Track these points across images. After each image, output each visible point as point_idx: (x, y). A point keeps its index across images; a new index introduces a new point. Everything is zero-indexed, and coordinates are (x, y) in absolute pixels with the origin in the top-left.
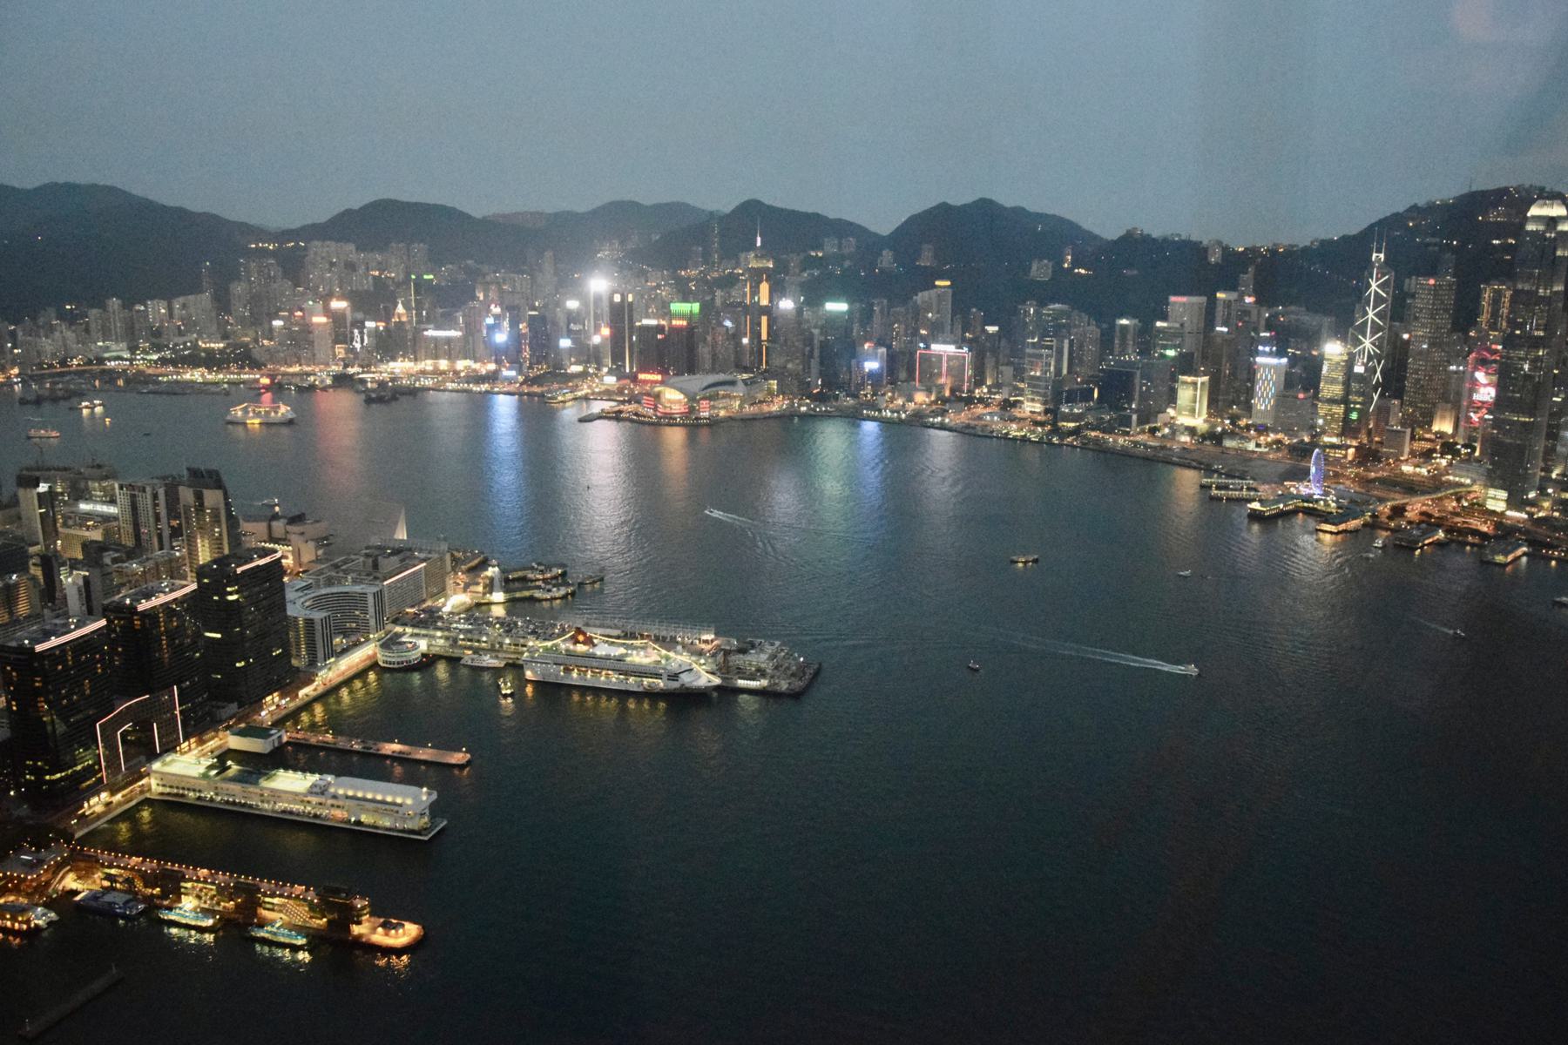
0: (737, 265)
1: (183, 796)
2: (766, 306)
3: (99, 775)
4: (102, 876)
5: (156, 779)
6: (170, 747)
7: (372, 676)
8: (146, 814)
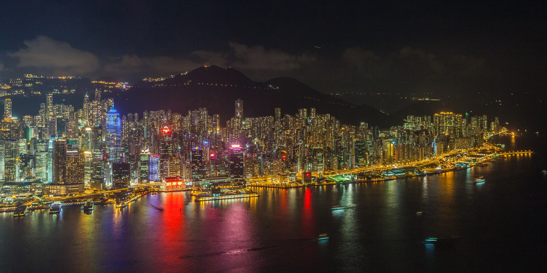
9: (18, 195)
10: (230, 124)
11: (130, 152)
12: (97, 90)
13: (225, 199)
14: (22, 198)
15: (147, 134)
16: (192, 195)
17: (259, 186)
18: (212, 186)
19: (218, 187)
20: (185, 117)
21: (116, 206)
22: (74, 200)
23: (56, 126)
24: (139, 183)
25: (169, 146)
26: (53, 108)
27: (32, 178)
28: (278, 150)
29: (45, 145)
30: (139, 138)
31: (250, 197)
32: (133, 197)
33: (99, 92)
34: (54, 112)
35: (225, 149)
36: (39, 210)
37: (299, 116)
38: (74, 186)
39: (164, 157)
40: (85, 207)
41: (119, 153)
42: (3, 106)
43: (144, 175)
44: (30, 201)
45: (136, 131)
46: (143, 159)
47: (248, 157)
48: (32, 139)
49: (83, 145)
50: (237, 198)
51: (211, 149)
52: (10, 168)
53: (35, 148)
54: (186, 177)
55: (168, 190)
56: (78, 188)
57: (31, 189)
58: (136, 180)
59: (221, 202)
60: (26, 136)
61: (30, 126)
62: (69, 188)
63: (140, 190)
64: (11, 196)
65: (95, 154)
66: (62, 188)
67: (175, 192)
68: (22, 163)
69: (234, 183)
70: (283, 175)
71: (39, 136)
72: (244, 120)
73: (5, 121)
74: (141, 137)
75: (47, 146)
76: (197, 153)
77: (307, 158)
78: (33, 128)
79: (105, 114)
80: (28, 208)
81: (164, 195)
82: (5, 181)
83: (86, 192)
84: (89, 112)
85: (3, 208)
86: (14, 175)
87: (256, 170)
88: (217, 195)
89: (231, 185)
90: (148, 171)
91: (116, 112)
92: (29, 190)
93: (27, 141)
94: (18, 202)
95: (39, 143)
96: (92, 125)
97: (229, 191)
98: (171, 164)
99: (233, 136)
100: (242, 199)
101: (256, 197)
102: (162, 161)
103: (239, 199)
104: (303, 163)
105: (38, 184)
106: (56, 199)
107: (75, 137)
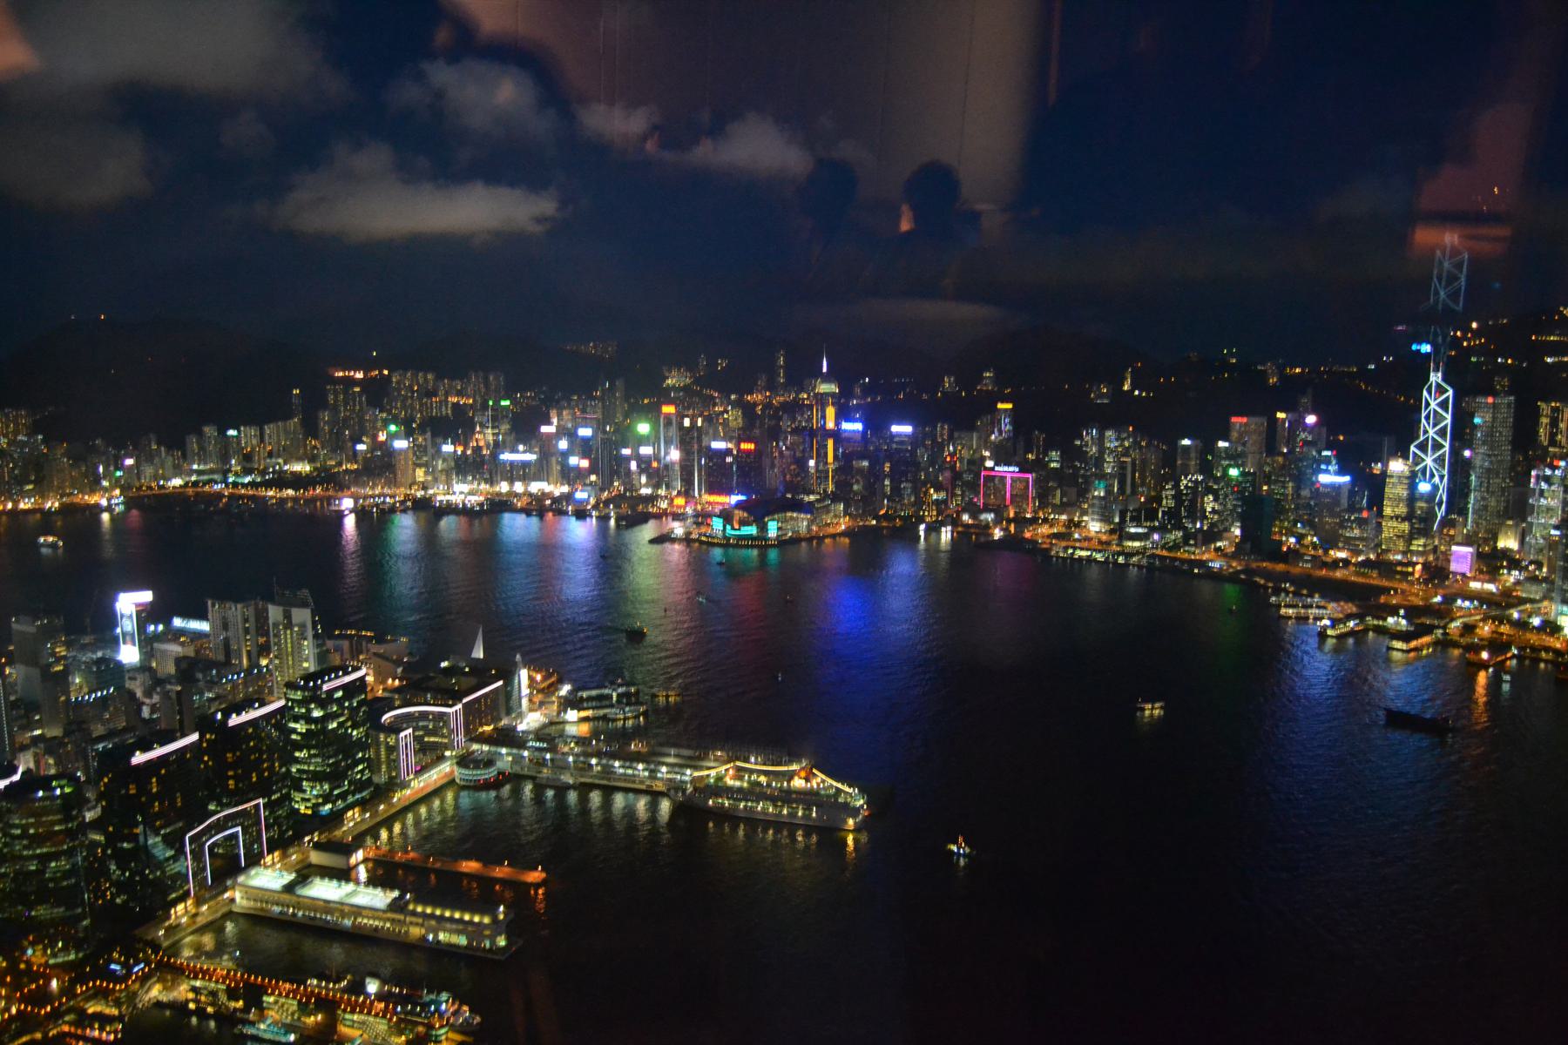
0: (802, 390)
1: (267, 911)
2: (833, 430)
3: (186, 888)
4: (189, 988)
5: (241, 892)
6: (254, 860)
7: (450, 796)
8: (229, 927)
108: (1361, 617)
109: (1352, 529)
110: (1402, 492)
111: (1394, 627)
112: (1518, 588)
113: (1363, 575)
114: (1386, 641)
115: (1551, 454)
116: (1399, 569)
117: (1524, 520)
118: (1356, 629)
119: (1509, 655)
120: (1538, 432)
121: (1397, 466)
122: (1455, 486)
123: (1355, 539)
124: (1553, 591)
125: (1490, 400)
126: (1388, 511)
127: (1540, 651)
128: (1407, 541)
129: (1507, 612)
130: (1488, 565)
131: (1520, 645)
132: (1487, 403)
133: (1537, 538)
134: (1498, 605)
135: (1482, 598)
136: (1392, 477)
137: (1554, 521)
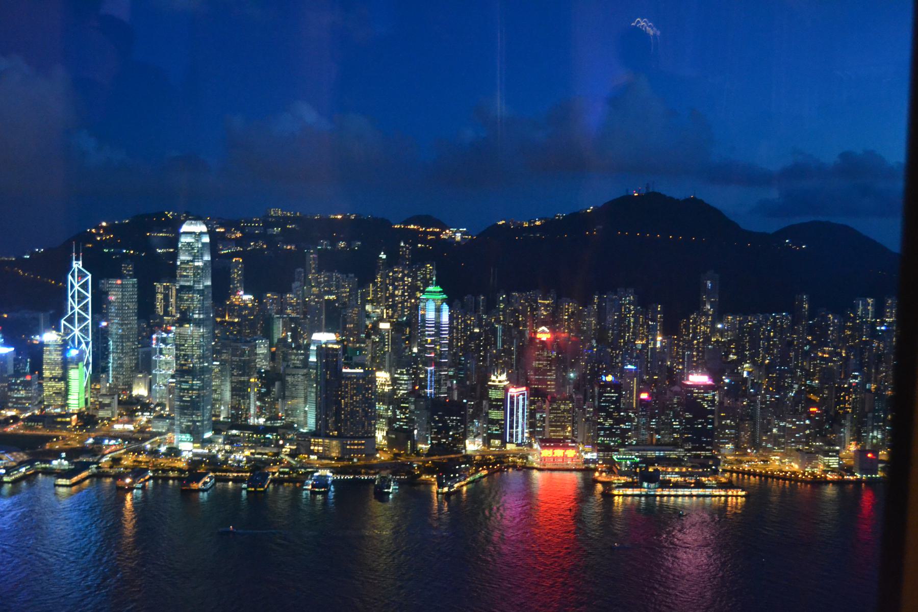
9: (253, 451)
10: (687, 327)
11: (468, 377)
12: (402, 244)
13: (669, 496)
14: (260, 456)
15: (504, 342)
16: (596, 481)
17: (749, 473)
18: (640, 465)
19: (655, 468)
20: (587, 308)
21: (438, 493)
22: (355, 470)
23: (323, 317)
24: (484, 445)
25: (550, 371)
26: (318, 278)
27: (278, 420)
28: (799, 392)
29: (302, 354)
30: (485, 350)
31: (727, 496)
32: (473, 474)
33: (407, 248)
34: (319, 287)
35: (673, 383)
36: (291, 484)
37: (856, 315)
38: (356, 442)
39: (537, 395)
40: (376, 487)
41: (444, 380)
42: (229, 273)
43: (495, 429)
44: (275, 463)
45: (479, 334)
46: (493, 394)
47: (725, 405)
48: (280, 340)
49: (373, 358)
50: (698, 496)
51: (641, 381)
52: (239, 396)
53: (285, 358)
54: (583, 440)
55: (545, 465)
56: (363, 447)
57: (277, 441)
58: (479, 441)
59: (661, 501)
60: (267, 334)
61: (277, 314)
62: (347, 444)
63: (486, 460)
64: (243, 452)
65: (398, 379)
66: (334, 443)
67: (561, 473)
68: (261, 387)
69: (691, 462)
70: (808, 453)
71: (291, 335)
72: (721, 321)
73: (232, 303)
74: (491, 348)
75: (307, 356)
76: (611, 390)
77: (870, 415)
78: (281, 320)
79: (418, 295)
80: (270, 477)
81: (536, 474)
82: (231, 422)
83: (378, 455)
84: (387, 289)
85: (228, 474)
86: (246, 411)
87: (745, 436)
88: (652, 485)
89: (684, 466)
90: (503, 422)
91: (440, 292)
92: (274, 442)
93: (271, 346)
94: (254, 465)
95: (293, 349)
96: (392, 317)
97: (680, 479)
98: (553, 409)
99: (693, 356)
100: (708, 500)
101: (742, 496)
102: (532, 403)
103: (701, 499)
104: (860, 428)
105: (289, 432)
106: (321, 465)
107: (360, 341)
108: (30, 463)
109: (19, 390)
110: (56, 357)
111: (58, 467)
112: (150, 425)
113: (31, 428)
114: (51, 480)
115: (166, 322)
116: (59, 419)
117: (150, 373)
118: (28, 473)
119: (147, 478)
120: (155, 305)
121: (50, 337)
122: (98, 349)
123: (21, 398)
124: (174, 424)
125: (119, 282)
126: (47, 374)
127: (169, 470)
128: (64, 397)
129: (143, 445)
130: (127, 410)
131: (154, 469)
132: (117, 284)
133: (160, 387)
134: (136, 440)
135: (124, 437)
136: (48, 345)
137: (171, 372)
